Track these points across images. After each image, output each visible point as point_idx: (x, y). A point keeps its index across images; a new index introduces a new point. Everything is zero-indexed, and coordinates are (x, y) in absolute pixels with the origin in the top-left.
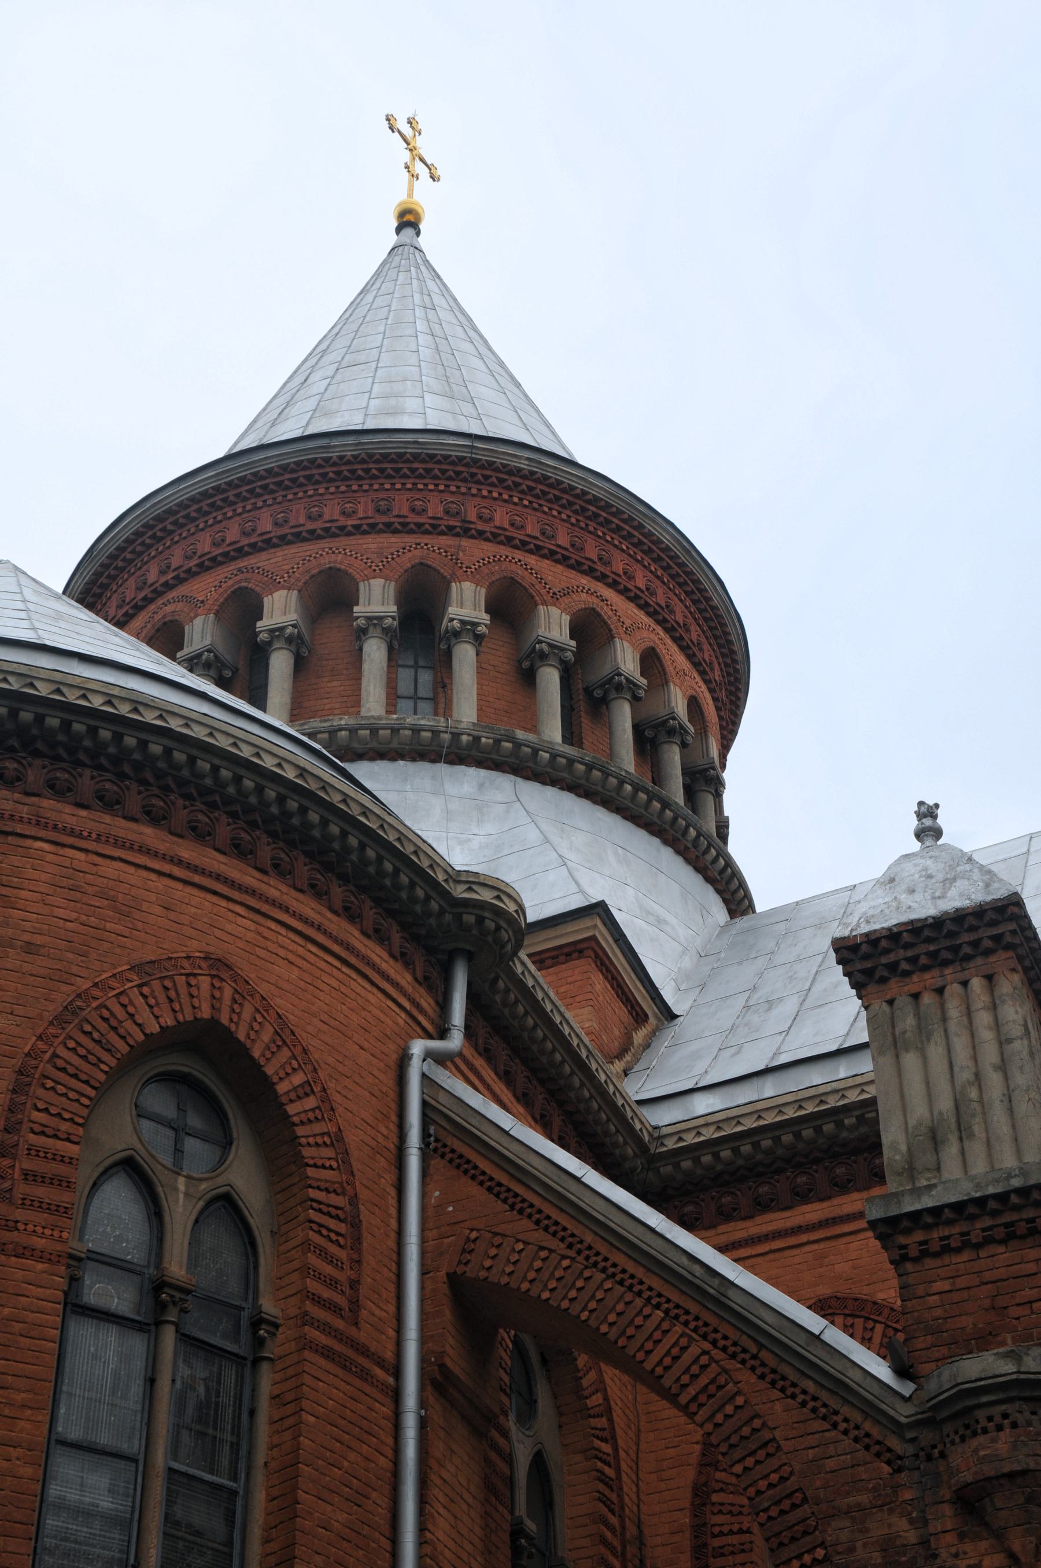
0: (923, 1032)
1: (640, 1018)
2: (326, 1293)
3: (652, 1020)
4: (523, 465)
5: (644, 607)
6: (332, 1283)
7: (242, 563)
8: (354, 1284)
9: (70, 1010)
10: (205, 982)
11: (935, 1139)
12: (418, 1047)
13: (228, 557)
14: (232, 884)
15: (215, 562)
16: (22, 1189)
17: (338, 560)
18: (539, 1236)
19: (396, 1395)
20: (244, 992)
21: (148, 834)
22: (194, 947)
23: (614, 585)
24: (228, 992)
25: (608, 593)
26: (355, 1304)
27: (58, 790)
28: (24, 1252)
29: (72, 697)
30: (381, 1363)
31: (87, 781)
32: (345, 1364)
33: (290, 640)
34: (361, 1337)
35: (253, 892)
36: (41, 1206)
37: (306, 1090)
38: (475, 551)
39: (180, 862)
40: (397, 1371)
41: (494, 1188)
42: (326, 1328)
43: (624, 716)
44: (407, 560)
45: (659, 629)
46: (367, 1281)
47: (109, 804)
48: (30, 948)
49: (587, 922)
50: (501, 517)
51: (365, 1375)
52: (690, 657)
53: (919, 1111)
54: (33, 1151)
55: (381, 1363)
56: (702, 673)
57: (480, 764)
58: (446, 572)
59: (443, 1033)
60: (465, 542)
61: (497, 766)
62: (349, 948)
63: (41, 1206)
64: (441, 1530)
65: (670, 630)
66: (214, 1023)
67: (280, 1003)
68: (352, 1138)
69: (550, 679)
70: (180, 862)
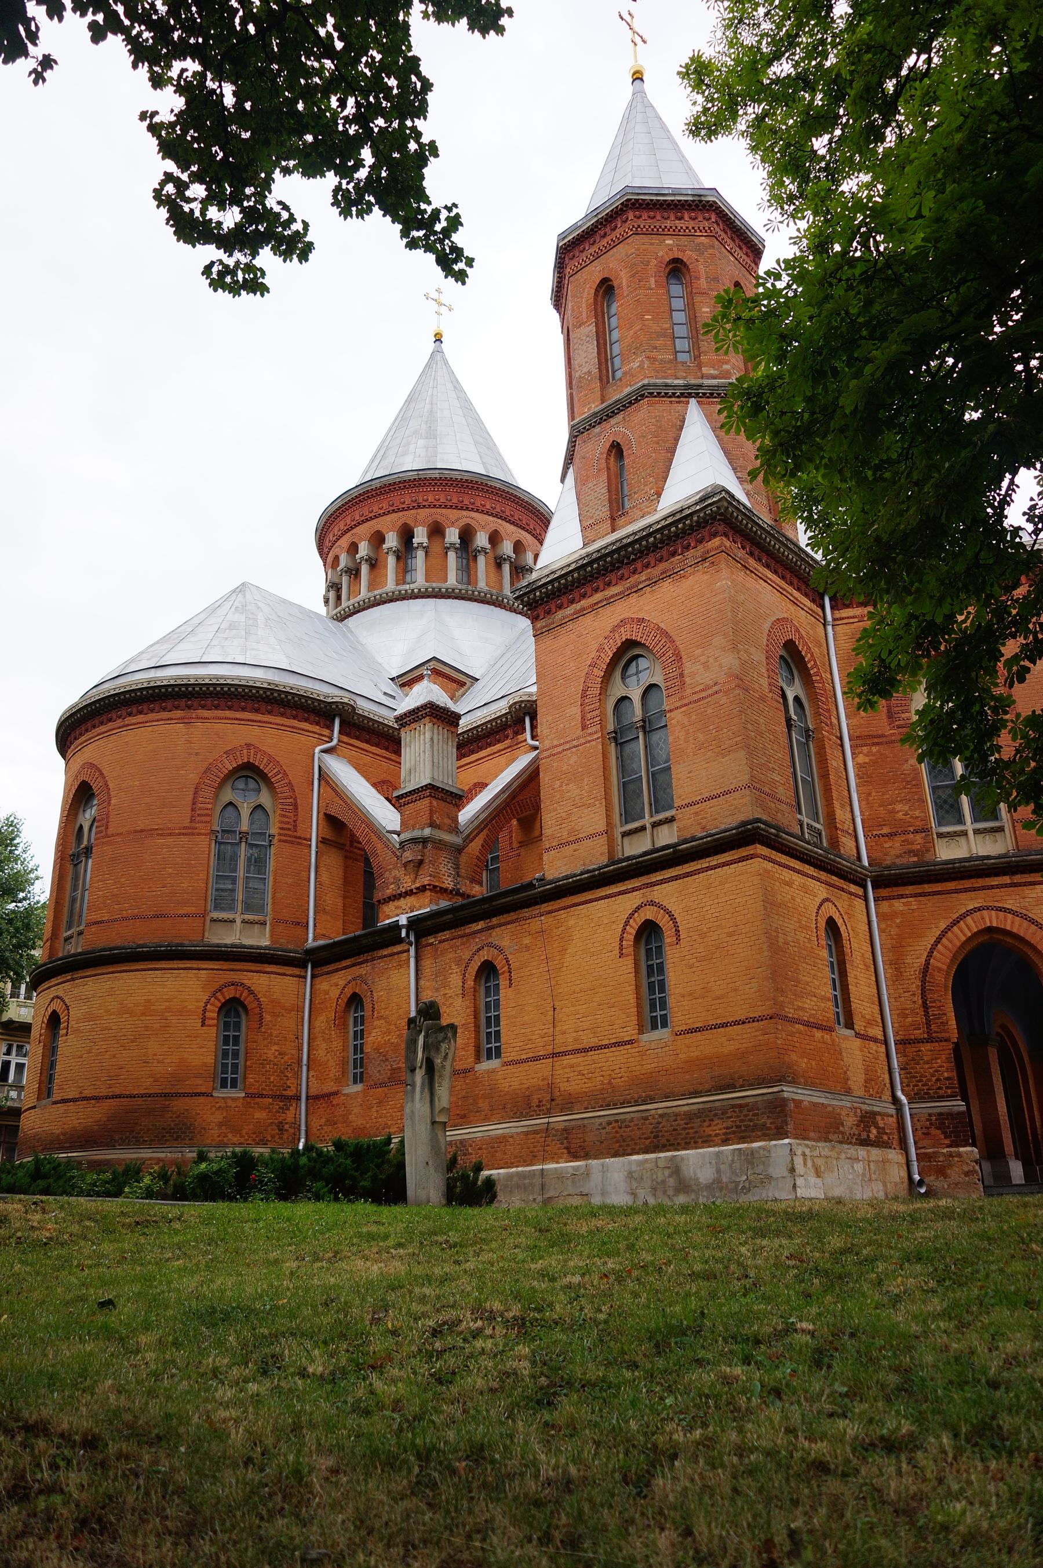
0: (410, 742)
1: (462, 684)
2: (286, 826)
3: (468, 684)
4: (437, 476)
5: (492, 515)
6: (288, 823)
7: (352, 532)
8: (295, 821)
9: (208, 769)
10: (245, 751)
12: (317, 750)
13: (349, 530)
14: (253, 721)
15: (346, 532)
16: (198, 819)
17: (378, 527)
18: (341, 802)
19: (310, 846)
20: (257, 750)
22: (242, 743)
23: (477, 511)
26: (295, 826)
27: (203, 707)
28: (200, 834)
29: (200, 681)
30: (305, 839)
31: (209, 702)
32: (292, 842)
33: (366, 560)
34: (298, 834)
35: (259, 721)
36: (202, 822)
37: (278, 773)
38: (423, 513)
39: (236, 719)
42: (286, 835)
43: (481, 560)
44: (400, 523)
45: (499, 521)
46: (300, 819)
47: (217, 707)
48: (197, 754)
49: (431, 663)
50: (431, 498)
51: (299, 844)
52: (517, 525)
54: (201, 809)
55: (305, 839)
56: (523, 529)
57: (422, 597)
58: (412, 525)
59: (332, 740)
60: (419, 511)
61: (429, 597)
62: (293, 727)
63: (202, 822)
64: (325, 877)
65: (505, 519)
66: (249, 762)
67: (269, 751)
68: (294, 782)
69: (452, 555)
70: (236, 719)
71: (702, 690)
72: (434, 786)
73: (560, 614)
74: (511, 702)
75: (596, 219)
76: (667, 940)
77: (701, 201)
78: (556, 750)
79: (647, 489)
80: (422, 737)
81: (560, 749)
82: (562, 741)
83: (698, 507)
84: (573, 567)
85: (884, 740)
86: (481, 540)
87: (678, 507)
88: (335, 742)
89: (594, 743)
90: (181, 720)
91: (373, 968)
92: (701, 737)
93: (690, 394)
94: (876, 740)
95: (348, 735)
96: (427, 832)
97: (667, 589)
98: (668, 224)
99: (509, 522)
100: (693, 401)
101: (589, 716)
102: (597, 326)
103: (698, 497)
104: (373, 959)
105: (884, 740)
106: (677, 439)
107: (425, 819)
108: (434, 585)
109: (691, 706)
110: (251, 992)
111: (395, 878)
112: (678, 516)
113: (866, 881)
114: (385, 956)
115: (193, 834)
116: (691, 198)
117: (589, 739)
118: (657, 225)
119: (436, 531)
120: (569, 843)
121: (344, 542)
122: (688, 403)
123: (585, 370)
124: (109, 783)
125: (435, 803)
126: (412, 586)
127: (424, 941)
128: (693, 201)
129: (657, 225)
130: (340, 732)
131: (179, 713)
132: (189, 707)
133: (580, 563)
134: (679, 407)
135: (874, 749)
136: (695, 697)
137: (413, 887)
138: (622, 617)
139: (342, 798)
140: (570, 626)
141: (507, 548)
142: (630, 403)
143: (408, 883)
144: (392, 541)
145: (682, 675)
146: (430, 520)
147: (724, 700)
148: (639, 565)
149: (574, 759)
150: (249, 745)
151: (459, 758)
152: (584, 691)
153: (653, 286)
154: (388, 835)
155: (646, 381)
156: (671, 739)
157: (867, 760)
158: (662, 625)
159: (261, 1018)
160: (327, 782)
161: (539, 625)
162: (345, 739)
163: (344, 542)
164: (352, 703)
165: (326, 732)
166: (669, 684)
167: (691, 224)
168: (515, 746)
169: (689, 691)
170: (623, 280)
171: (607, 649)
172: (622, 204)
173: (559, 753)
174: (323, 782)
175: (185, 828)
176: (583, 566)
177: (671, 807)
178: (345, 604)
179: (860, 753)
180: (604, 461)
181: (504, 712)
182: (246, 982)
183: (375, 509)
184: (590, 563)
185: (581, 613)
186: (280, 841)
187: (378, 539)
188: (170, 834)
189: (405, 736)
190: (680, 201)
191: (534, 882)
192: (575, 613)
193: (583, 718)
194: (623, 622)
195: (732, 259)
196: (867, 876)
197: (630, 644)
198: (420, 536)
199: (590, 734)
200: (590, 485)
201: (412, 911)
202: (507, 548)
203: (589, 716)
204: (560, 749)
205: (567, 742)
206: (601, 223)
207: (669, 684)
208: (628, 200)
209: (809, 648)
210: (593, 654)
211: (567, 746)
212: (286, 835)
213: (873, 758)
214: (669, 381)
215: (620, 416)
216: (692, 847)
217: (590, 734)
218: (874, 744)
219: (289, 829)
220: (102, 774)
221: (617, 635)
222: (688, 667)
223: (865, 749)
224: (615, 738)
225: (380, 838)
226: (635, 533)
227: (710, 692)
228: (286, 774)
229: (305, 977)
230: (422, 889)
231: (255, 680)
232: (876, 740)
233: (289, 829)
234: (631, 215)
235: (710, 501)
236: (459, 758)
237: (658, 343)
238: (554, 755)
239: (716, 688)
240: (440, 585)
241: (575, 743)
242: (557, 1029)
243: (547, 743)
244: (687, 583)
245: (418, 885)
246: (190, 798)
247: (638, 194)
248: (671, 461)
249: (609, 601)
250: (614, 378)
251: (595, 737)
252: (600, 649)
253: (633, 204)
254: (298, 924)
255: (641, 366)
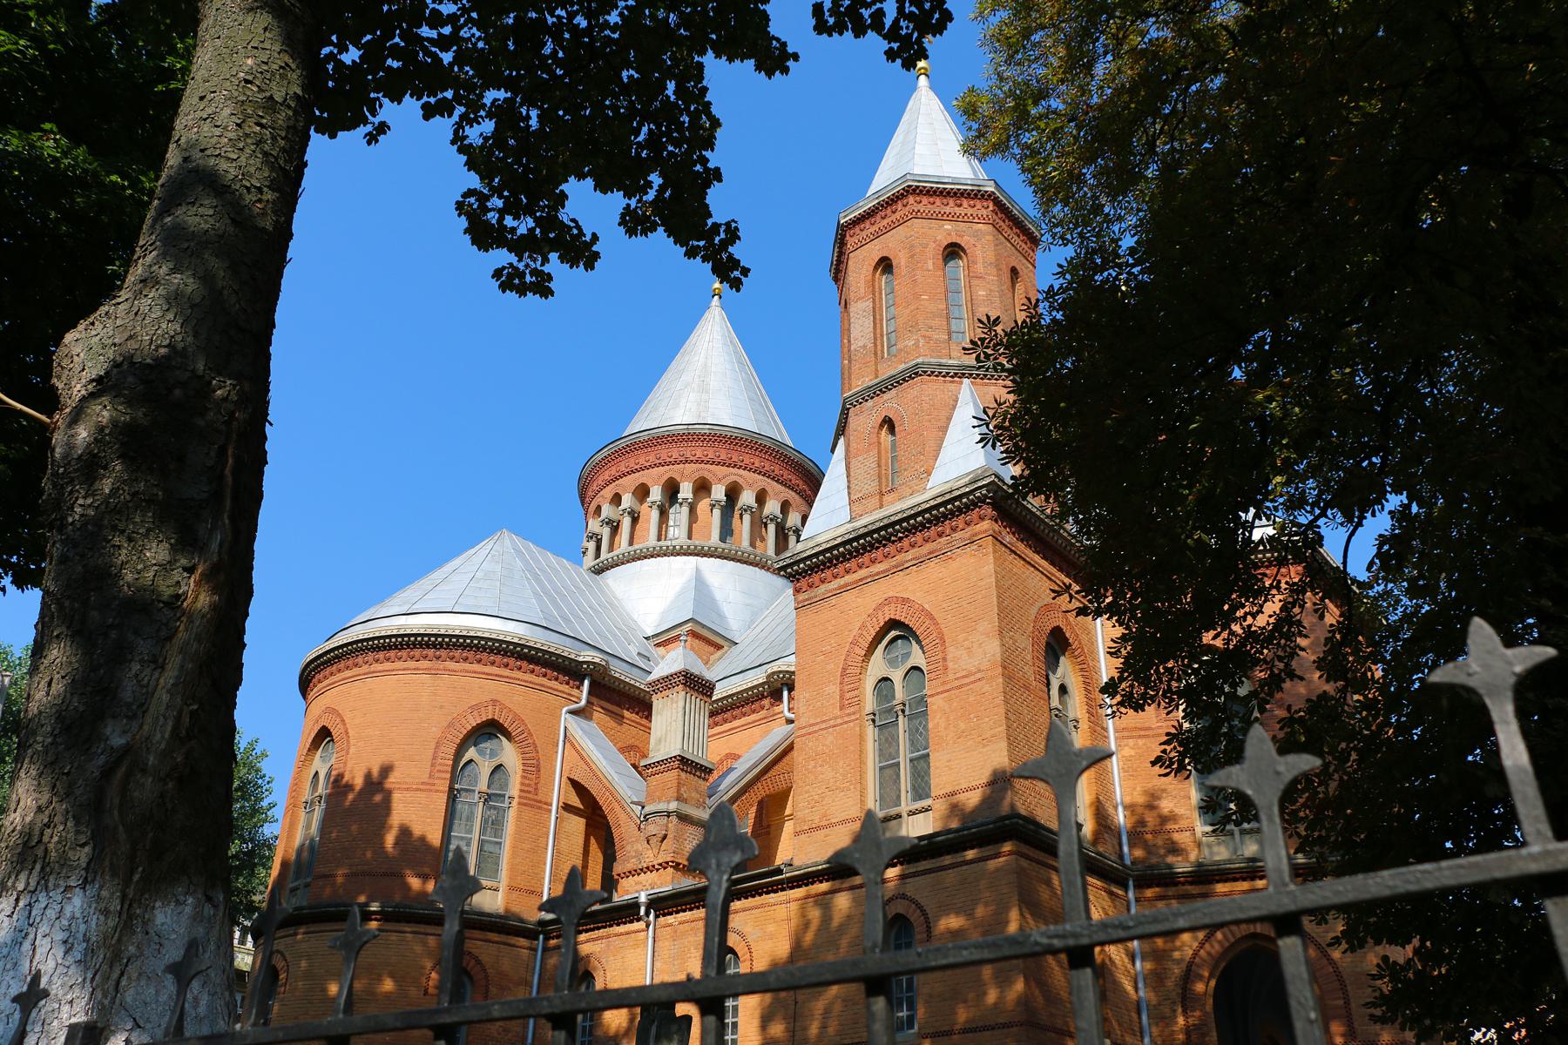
2: (526, 789)
4: (708, 432)
6: (529, 785)
11: (660, 741)
12: (564, 710)
14: (501, 676)
16: (437, 775)
19: (550, 811)
21: (476, 667)
22: (488, 698)
24: (497, 708)
25: (741, 472)
26: (536, 789)
28: (437, 791)
30: (546, 804)
32: (532, 806)
34: (539, 798)
38: (690, 467)
40: (551, 805)
41: (578, 752)
42: (526, 798)
44: (665, 478)
48: (441, 707)
50: (699, 453)
51: (540, 808)
53: (659, 734)
54: (440, 764)
55: (546, 804)
58: (678, 480)
62: (542, 685)
65: (773, 479)
66: (493, 720)
67: (515, 708)
71: (963, 677)
72: (683, 758)
73: (823, 588)
74: (769, 671)
75: (877, 201)
76: (918, 937)
77: (979, 191)
78: (812, 729)
79: (918, 467)
80: (674, 705)
81: (816, 728)
82: (818, 720)
83: (967, 490)
84: (839, 540)
85: (1150, 733)
86: (747, 498)
87: (947, 487)
88: (583, 702)
89: (852, 724)
90: (428, 671)
91: (608, 946)
92: (962, 726)
93: (963, 374)
94: (1142, 733)
95: (597, 696)
96: (673, 806)
97: (934, 570)
98: (948, 210)
99: (777, 481)
100: (966, 381)
101: (848, 695)
102: (874, 302)
103: (967, 479)
104: (608, 937)
105: (1150, 733)
106: (949, 419)
107: (672, 793)
108: (697, 543)
109: (953, 692)
110: (479, 962)
111: (636, 851)
112: (948, 497)
113: (1128, 880)
114: (622, 934)
115: (431, 790)
116: (970, 188)
117: (846, 719)
118: (937, 210)
119: (702, 487)
120: (818, 828)
121: (608, 493)
122: (962, 383)
123: (861, 344)
124: (349, 731)
125: (683, 775)
126: (674, 543)
127: (662, 919)
128: (972, 191)
129: (937, 210)
130: (590, 693)
131: (424, 664)
132: (438, 658)
133: (847, 537)
134: (952, 387)
135: (1140, 742)
136: (957, 683)
137: (655, 863)
138: (886, 596)
139: (587, 764)
140: (834, 601)
141: (772, 507)
142: (904, 380)
143: (650, 857)
144: (656, 494)
145: (944, 659)
146: (697, 476)
147: (987, 688)
148: (906, 542)
149: (831, 738)
150: (494, 702)
151: (710, 727)
152: (844, 669)
153: (931, 268)
154: (634, 807)
155: (920, 360)
156: (930, 725)
157: (1133, 753)
158: (926, 606)
159: (487, 991)
160: (573, 745)
161: (801, 597)
162: (594, 700)
163: (608, 493)
164: (604, 663)
165: (575, 692)
166: (930, 668)
167: (970, 211)
168: (770, 719)
169: (951, 676)
170: (900, 261)
171: (869, 627)
172: (903, 189)
173: (815, 732)
174: (567, 745)
175: (423, 783)
176: (850, 541)
177: (928, 796)
178: (604, 555)
179: (1125, 745)
180: (875, 435)
181: (761, 681)
182: (473, 951)
183: (642, 461)
184: (856, 539)
185: (845, 589)
186: (519, 804)
187: (642, 492)
188: (407, 789)
189: (658, 703)
190: (959, 190)
191: (782, 867)
192: (840, 588)
193: (842, 697)
194: (888, 601)
195: (1009, 245)
196: (1129, 875)
197: (893, 624)
198: (686, 491)
199: (849, 715)
200: (860, 458)
201: (652, 888)
202: (772, 507)
203: (848, 695)
204: (816, 728)
205: (824, 721)
206: (882, 206)
207: (930, 668)
208: (909, 186)
209: (1077, 635)
210: (855, 632)
211: (824, 726)
212: (526, 798)
213: (1140, 751)
214: (943, 361)
215: (894, 391)
216: (948, 840)
217: (849, 715)
218: (1140, 737)
219: (529, 792)
220: (343, 721)
221: (880, 613)
222: (952, 652)
223: (1131, 742)
224: (873, 721)
225: (623, 808)
226: (903, 511)
227: (972, 678)
228: (530, 734)
229: (535, 950)
230: (664, 866)
231: (506, 633)
232: (1142, 733)
233: (529, 792)
234: (911, 199)
235: (980, 484)
236: (710, 727)
237: (932, 323)
238: (809, 734)
239: (979, 675)
240: (703, 543)
241: (832, 723)
242: (798, 1024)
243: (802, 722)
244: (954, 565)
245: (660, 861)
246: (430, 753)
247: (919, 181)
248: (942, 440)
249: (875, 578)
250: (888, 354)
251: (853, 717)
252: (863, 626)
253: (914, 190)
254: (533, 892)
255: (916, 345)
